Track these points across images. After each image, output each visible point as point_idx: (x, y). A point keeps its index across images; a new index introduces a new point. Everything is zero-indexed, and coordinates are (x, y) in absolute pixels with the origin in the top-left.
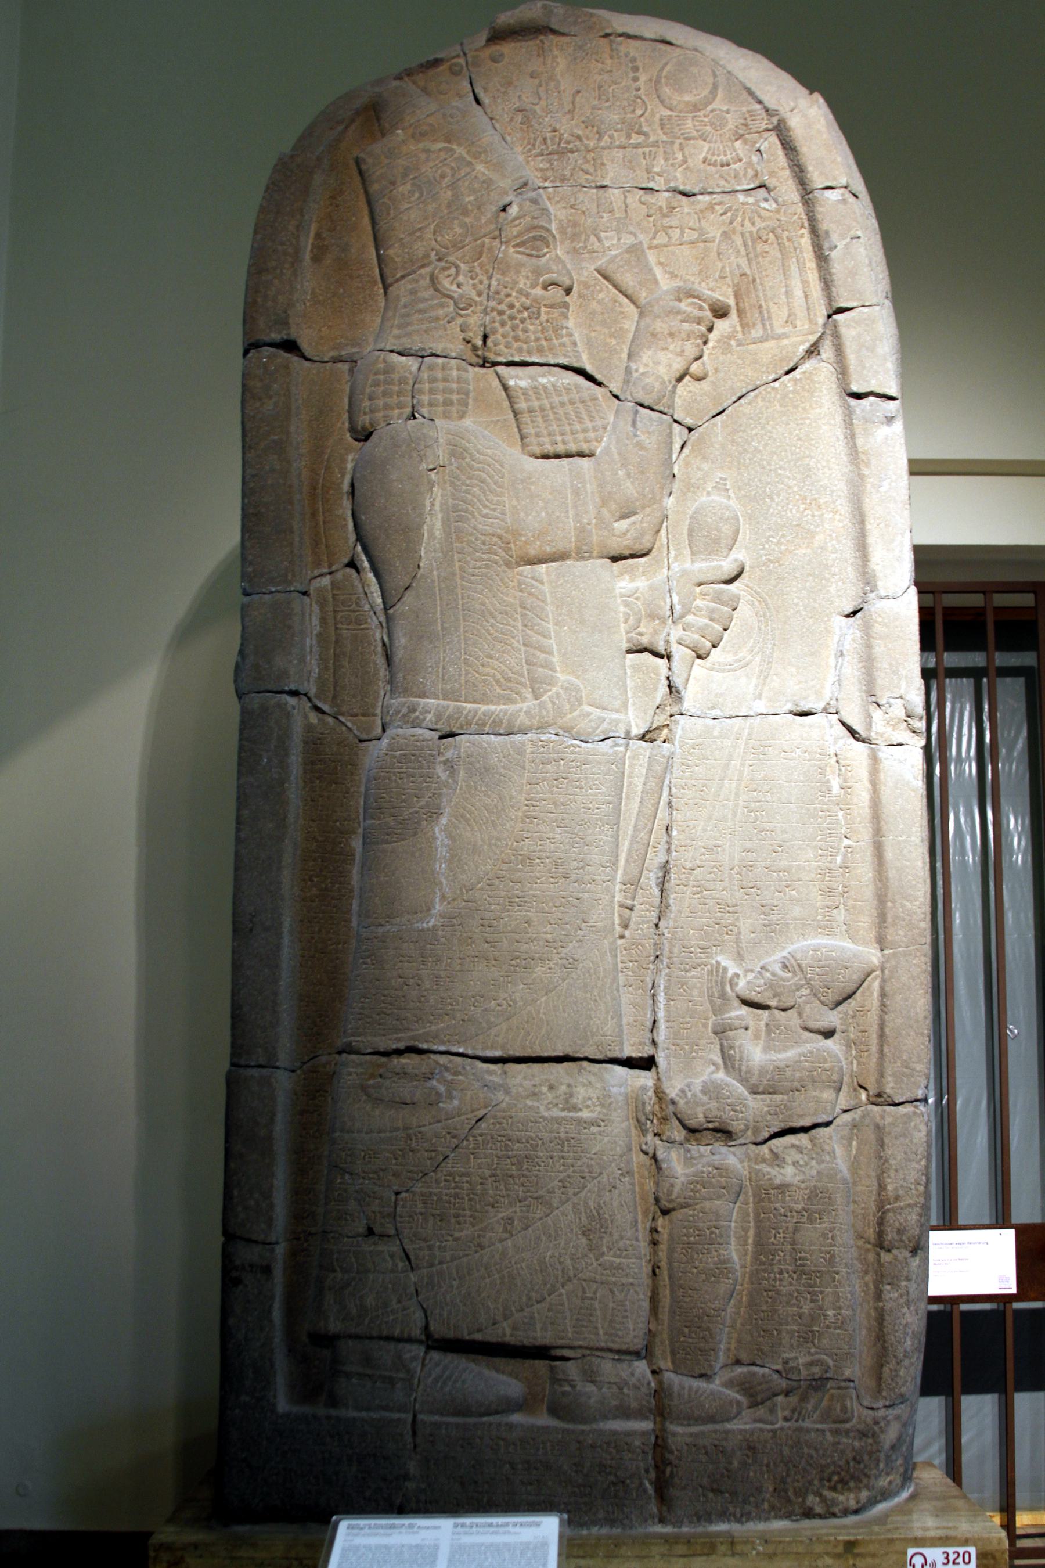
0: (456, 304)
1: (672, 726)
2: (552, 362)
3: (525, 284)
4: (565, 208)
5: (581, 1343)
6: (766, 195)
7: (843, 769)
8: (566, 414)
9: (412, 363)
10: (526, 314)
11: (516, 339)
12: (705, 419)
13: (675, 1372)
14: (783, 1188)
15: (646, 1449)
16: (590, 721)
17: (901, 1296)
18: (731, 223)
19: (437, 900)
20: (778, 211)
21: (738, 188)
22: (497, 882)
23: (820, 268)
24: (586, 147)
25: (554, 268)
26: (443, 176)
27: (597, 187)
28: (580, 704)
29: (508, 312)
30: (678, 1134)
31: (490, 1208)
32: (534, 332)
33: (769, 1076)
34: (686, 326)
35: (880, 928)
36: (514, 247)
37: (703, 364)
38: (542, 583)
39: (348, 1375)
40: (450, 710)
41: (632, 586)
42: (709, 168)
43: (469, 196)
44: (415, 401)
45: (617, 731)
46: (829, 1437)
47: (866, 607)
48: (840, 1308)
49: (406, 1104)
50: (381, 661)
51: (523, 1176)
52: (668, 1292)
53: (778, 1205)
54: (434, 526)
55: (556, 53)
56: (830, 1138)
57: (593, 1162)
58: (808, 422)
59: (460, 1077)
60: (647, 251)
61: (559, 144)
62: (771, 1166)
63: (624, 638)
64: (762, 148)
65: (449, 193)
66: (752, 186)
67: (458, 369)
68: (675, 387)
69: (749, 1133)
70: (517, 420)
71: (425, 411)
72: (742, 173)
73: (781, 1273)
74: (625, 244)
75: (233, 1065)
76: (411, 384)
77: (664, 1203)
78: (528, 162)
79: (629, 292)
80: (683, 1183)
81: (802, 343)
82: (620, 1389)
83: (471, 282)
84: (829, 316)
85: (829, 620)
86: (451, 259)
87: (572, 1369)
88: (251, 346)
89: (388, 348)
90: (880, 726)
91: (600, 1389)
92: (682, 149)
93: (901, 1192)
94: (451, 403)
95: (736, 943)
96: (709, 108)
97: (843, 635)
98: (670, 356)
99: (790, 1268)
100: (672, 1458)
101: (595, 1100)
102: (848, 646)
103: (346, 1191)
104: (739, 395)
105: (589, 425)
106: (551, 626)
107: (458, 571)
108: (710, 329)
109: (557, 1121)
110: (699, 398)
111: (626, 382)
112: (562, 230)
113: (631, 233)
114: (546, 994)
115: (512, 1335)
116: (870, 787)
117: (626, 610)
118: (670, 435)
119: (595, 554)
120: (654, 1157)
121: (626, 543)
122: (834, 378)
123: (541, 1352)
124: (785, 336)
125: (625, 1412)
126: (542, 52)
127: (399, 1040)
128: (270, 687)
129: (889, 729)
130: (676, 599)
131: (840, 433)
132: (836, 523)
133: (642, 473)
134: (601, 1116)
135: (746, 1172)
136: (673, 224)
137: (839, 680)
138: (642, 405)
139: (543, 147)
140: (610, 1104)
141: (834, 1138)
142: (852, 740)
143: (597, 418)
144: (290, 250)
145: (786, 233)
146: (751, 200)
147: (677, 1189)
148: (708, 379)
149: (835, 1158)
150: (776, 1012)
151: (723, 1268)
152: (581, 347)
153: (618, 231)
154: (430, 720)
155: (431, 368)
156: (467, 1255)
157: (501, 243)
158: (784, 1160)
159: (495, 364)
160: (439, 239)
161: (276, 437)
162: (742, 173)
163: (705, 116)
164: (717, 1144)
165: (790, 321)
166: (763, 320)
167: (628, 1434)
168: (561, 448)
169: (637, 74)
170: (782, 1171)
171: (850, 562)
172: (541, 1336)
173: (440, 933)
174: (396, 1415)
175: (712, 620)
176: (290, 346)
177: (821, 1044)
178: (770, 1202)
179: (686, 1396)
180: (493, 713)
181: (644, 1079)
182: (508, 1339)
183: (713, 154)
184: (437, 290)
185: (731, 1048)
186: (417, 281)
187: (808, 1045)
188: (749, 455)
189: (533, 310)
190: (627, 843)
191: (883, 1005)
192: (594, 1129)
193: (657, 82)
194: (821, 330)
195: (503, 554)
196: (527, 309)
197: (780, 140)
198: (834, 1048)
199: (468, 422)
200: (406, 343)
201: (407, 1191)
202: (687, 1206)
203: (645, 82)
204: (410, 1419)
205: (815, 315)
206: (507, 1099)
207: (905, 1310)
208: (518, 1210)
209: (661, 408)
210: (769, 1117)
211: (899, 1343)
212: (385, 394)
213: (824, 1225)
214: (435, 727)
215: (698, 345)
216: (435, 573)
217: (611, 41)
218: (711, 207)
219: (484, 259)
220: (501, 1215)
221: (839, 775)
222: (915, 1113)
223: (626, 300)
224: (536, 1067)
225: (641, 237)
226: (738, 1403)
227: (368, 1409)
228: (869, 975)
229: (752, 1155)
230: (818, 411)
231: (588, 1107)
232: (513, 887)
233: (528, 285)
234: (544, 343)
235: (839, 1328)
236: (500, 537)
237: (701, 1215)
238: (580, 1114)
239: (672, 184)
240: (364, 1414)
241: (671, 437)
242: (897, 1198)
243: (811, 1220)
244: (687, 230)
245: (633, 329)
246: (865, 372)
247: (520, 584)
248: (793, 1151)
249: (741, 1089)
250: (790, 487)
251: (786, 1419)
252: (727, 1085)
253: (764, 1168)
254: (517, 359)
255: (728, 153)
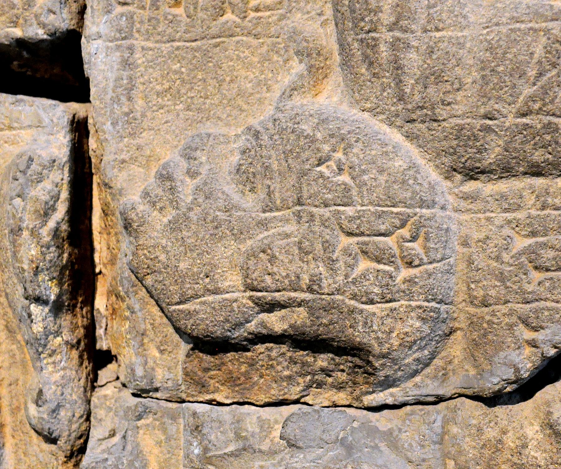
33: (528, 91)
164: (321, 398)
249: (407, 154)
252: (342, 140)
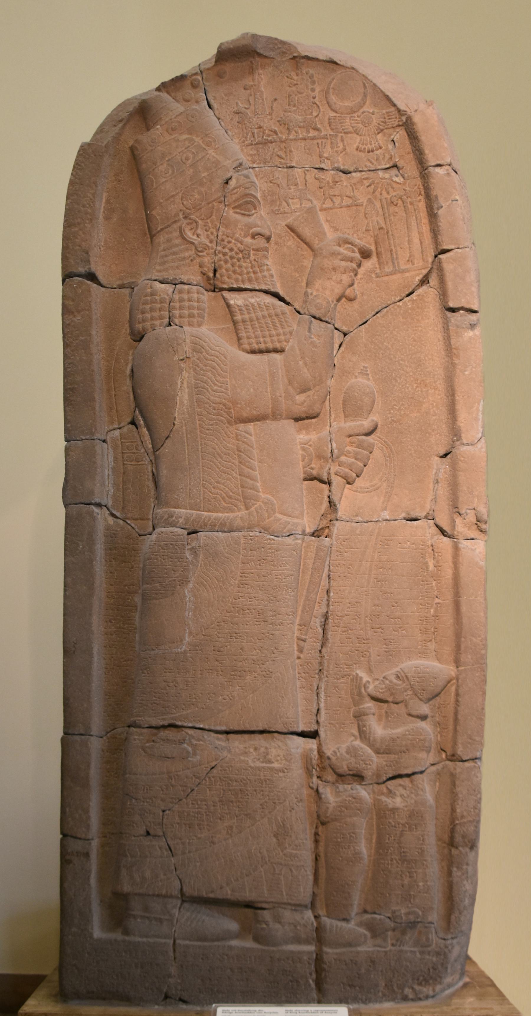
0: (196, 248)
1: (331, 528)
2: (257, 288)
3: (240, 234)
4: (266, 182)
5: (272, 900)
6: (397, 172)
7: (436, 554)
8: (266, 323)
9: (169, 288)
10: (240, 256)
11: (234, 272)
12: (355, 327)
13: (328, 917)
14: (394, 810)
15: (311, 962)
16: (280, 524)
17: (463, 874)
18: (374, 192)
19: (187, 634)
20: (404, 184)
21: (379, 167)
22: (223, 624)
23: (431, 222)
24: (280, 138)
25: (259, 223)
26: (187, 159)
27: (287, 167)
28: (274, 512)
29: (230, 254)
30: (331, 777)
31: (219, 821)
32: (246, 268)
34: (343, 263)
35: (457, 654)
36: (233, 208)
37: (354, 289)
38: (251, 435)
39: (135, 917)
40: (194, 516)
41: (307, 437)
42: (360, 154)
43: (204, 172)
44: (171, 314)
45: (297, 530)
46: (418, 955)
47: (454, 451)
48: (427, 881)
49: (168, 758)
50: (151, 485)
51: (239, 801)
52: (324, 870)
53: (391, 821)
54: (183, 397)
55: (261, 71)
56: (423, 781)
57: (280, 794)
58: (420, 329)
59: (201, 743)
60: (319, 212)
61: (263, 137)
62: (387, 796)
63: (302, 471)
64: (395, 139)
65: (191, 170)
66: (388, 166)
67: (198, 293)
68: (336, 305)
69: (375, 777)
70: (235, 327)
71: (177, 321)
72: (381, 157)
73: (392, 860)
74: (305, 207)
75: (65, 733)
76: (168, 303)
77: (323, 818)
78: (242, 150)
79: (308, 240)
80: (334, 807)
81: (418, 275)
82: (295, 926)
83: (206, 233)
84: (436, 256)
85: (430, 459)
86: (193, 217)
87: (267, 915)
88: (67, 276)
89: (153, 278)
90: (461, 527)
91: (283, 926)
92: (342, 140)
93: (465, 814)
94: (194, 316)
95: (368, 662)
96: (361, 111)
97: (438, 470)
98: (333, 283)
99: (397, 858)
100: (325, 966)
101: (282, 757)
102: (441, 476)
103: (133, 809)
104: (377, 310)
105: (281, 331)
106: (256, 463)
107: (198, 427)
108: (359, 265)
109: (259, 769)
110: (351, 313)
111: (305, 302)
112: (264, 197)
113: (309, 200)
114: (253, 693)
115: (231, 895)
116: (453, 566)
117: (303, 453)
118: (333, 336)
119: (284, 416)
120: (317, 791)
121: (303, 409)
122: (438, 299)
123: (249, 905)
124: (407, 271)
125: (298, 940)
126: (252, 71)
127: (164, 719)
128: (83, 501)
129: (466, 529)
130: (334, 445)
131: (440, 336)
132: (436, 398)
133: (314, 362)
134: (286, 767)
135: (372, 801)
136: (336, 193)
137: (435, 498)
138: (314, 317)
139: (252, 139)
140: (291, 759)
141: (425, 781)
142: (442, 537)
143: (286, 326)
144: (89, 211)
145: (409, 200)
146: (387, 176)
147: (330, 811)
148: (357, 300)
149: (426, 793)
150: (392, 704)
151: (357, 857)
152: (275, 279)
153: (300, 198)
154: (182, 523)
155: (180, 292)
156: (205, 848)
157: (225, 205)
158: (395, 794)
159: (222, 289)
160: (185, 203)
161: (83, 338)
162: (381, 157)
163: (358, 117)
165: (410, 261)
166: (392, 260)
167: (299, 952)
168: (263, 346)
169: (314, 87)
170: (394, 800)
171: (444, 421)
172: (248, 895)
173: (188, 654)
174: (163, 941)
175: (356, 459)
176: (92, 277)
177: (419, 724)
178: (386, 818)
179: (334, 932)
180: (220, 518)
181: (312, 744)
182: (229, 897)
183: (363, 144)
184: (184, 238)
185: (365, 726)
186: (171, 233)
187: (410, 725)
188: (382, 351)
189: (245, 253)
190: (302, 600)
191: (457, 701)
192: (281, 774)
193: (327, 92)
194: (430, 266)
195: (227, 416)
196: (242, 251)
197: (407, 133)
198: (429, 729)
199: (204, 329)
200: (164, 275)
201: (169, 810)
202: (335, 820)
203: (319, 92)
204: (172, 942)
205: (427, 256)
206: (229, 756)
207: (465, 882)
208: (235, 821)
209: (327, 319)
210: (386, 768)
211: (461, 901)
212: (152, 310)
213: (418, 833)
214: (185, 527)
215: (351, 276)
216: (184, 428)
217: (297, 61)
218: (361, 181)
219: (214, 217)
220: (226, 824)
221: (434, 558)
222: (475, 766)
223: (305, 245)
224: (246, 736)
225: (315, 202)
226: (365, 935)
227: (147, 937)
228: (449, 682)
229: (376, 790)
230: (427, 321)
231: (277, 761)
232: (232, 627)
233: (243, 235)
234: (252, 275)
235: (426, 893)
236: (224, 405)
237: (344, 825)
238: (273, 765)
239: (336, 165)
240: (145, 940)
241: (333, 339)
242: (463, 817)
243: (410, 829)
244: (345, 198)
245: (310, 266)
246: (458, 294)
247: (237, 435)
248: (401, 789)
249: (369, 751)
250: (407, 373)
251: (393, 945)
252: (361, 748)
253: (384, 798)
254: (235, 286)
255: (373, 142)
